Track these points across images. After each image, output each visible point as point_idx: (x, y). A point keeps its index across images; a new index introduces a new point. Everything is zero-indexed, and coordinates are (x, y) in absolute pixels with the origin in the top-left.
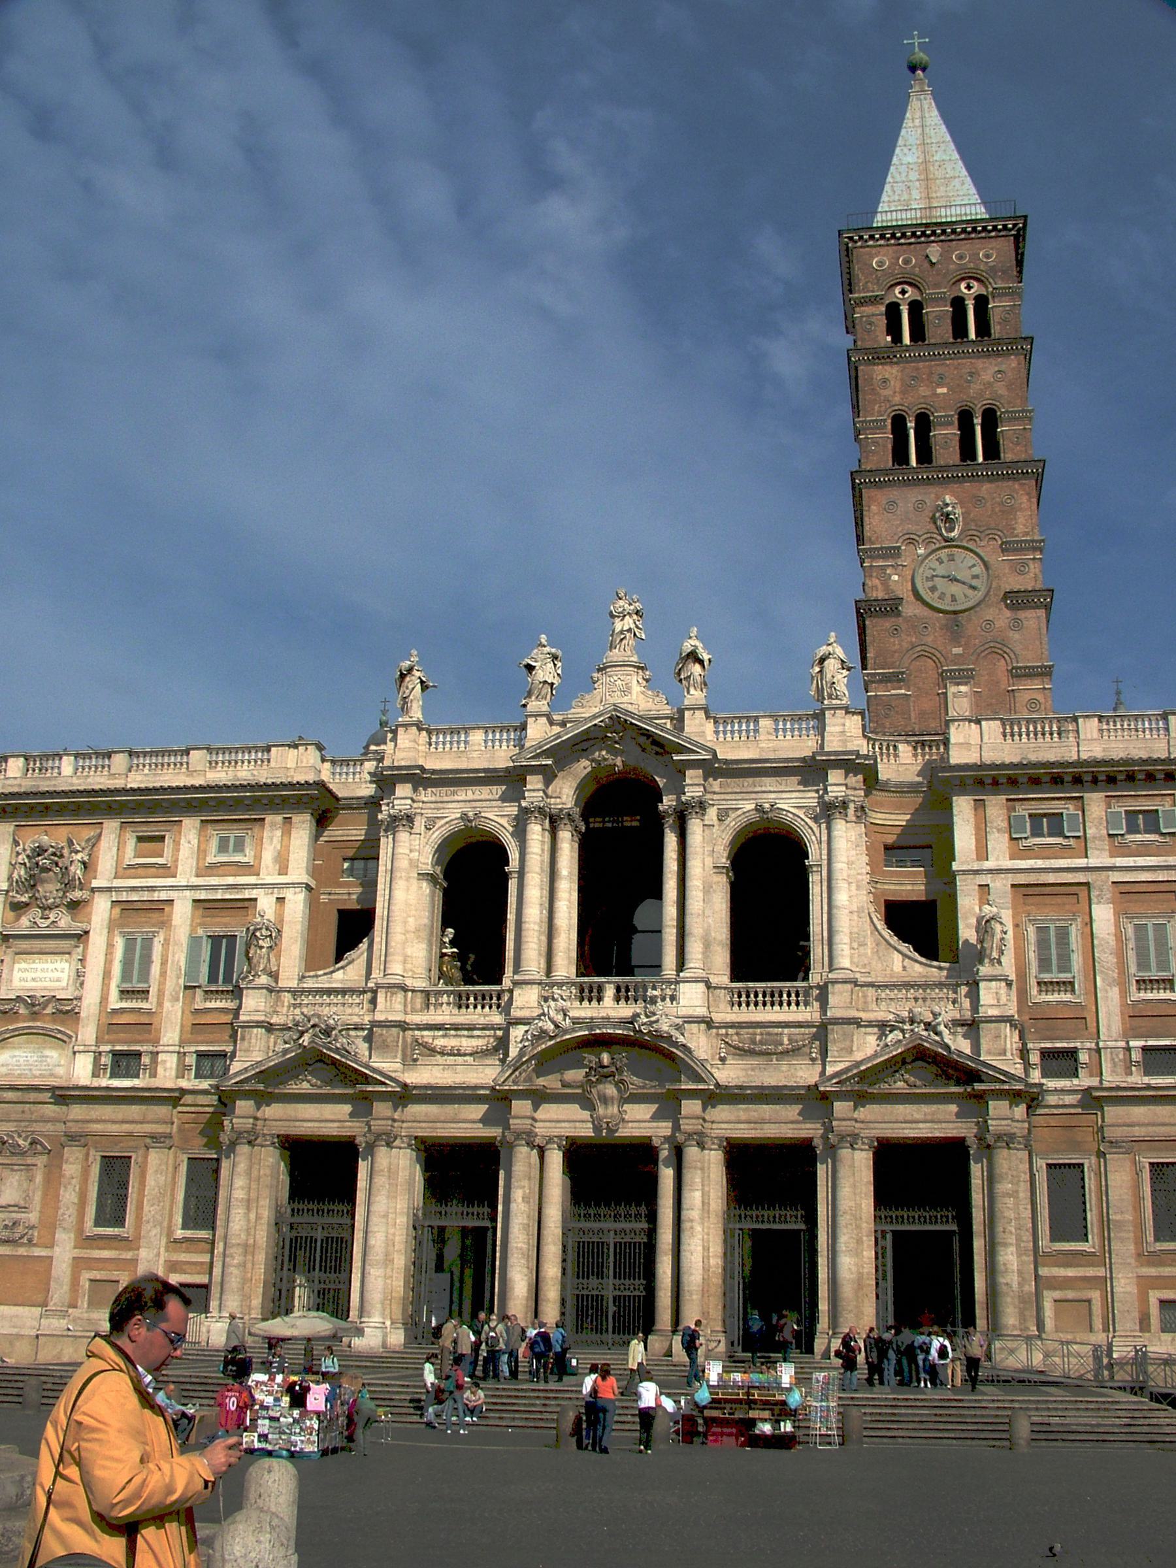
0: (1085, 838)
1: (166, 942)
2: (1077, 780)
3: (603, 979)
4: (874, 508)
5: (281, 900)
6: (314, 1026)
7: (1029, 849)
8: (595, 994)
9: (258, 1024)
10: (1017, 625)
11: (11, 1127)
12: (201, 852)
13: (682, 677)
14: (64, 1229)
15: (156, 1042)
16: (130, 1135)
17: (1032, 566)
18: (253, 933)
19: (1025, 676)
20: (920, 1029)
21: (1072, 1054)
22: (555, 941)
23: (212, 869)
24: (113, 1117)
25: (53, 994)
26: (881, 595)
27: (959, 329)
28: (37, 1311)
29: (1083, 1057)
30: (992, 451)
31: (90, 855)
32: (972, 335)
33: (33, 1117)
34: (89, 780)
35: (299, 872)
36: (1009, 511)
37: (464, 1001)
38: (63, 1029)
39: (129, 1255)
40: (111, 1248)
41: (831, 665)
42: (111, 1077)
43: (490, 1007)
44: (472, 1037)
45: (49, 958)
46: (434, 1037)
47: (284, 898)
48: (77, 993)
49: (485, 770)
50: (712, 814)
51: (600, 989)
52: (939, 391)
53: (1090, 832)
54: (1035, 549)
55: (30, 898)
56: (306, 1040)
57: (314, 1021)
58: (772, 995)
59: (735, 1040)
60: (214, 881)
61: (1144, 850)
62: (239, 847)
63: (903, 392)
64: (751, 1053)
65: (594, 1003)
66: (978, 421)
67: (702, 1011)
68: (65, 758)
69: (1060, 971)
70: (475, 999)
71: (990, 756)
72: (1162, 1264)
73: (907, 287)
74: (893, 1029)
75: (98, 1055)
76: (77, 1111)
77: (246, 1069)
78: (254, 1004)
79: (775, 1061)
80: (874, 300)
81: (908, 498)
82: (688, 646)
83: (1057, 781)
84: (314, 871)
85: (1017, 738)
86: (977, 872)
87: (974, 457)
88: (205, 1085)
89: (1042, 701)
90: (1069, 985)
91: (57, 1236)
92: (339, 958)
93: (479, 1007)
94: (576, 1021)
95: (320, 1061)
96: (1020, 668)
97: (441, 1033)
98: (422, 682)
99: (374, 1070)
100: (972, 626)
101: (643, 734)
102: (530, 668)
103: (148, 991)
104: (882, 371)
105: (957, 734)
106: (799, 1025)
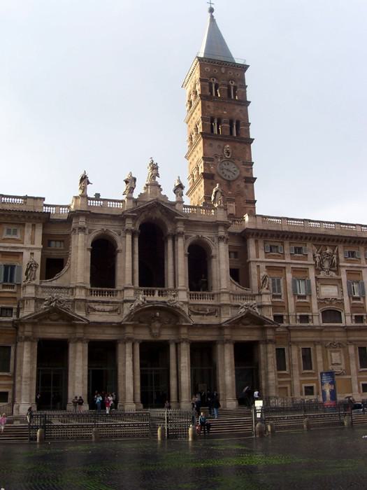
2: (283, 237)
3: (154, 288)
5: (32, 254)
6: (56, 300)
9: (33, 298)
10: (246, 187)
18: (31, 266)
20: (251, 309)
21: (281, 317)
23: (4, 239)
26: (208, 172)
29: (285, 318)
32: (233, 97)
35: (38, 244)
41: (219, 194)
52: (225, 112)
53: (286, 252)
56: (53, 304)
59: (192, 309)
60: (7, 245)
61: (298, 258)
62: (15, 233)
63: (214, 111)
64: (198, 314)
66: (235, 124)
67: (186, 300)
71: (259, 227)
74: (242, 307)
77: (31, 315)
78: (30, 292)
80: (206, 81)
81: (216, 144)
83: (278, 236)
84: (43, 243)
86: (256, 262)
90: (280, 297)
94: (148, 302)
99: (78, 316)
104: (208, 103)
106: (212, 305)
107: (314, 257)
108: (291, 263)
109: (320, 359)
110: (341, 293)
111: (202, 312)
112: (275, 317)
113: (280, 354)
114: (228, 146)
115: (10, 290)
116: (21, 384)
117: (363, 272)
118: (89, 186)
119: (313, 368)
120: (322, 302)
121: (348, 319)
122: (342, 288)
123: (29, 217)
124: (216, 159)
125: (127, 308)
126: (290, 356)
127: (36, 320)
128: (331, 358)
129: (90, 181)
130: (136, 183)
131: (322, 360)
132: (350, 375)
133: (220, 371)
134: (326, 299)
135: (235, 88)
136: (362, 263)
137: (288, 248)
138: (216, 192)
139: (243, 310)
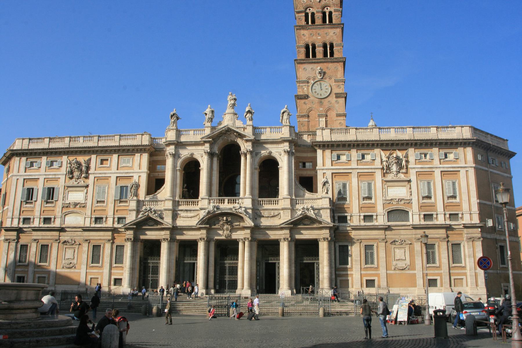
0: (351, 160)
4: (300, 70)
6: (149, 210)
7: (336, 163)
8: (223, 201)
9: (134, 210)
11: (69, 238)
13: (246, 117)
14: (84, 264)
15: (107, 214)
16: (100, 240)
17: (342, 86)
19: (339, 116)
22: (213, 187)
24: (96, 235)
25: (78, 202)
26: (301, 94)
27: (324, 21)
28: (77, 286)
30: (332, 54)
32: (327, 22)
33: (75, 235)
34: (87, 144)
36: (337, 70)
37: (188, 203)
39: (101, 271)
40: (96, 269)
41: (285, 114)
42: (95, 224)
43: (196, 205)
45: (78, 192)
46: (181, 213)
49: (195, 142)
50: (254, 153)
51: (224, 201)
52: (318, 38)
54: (342, 82)
56: (147, 213)
57: (148, 209)
58: (269, 202)
60: (122, 171)
61: (367, 163)
62: (128, 162)
63: (309, 38)
65: (223, 203)
66: (328, 46)
68: (81, 138)
70: (192, 203)
72: (367, 271)
73: (311, 9)
74: (300, 210)
76: (86, 233)
77: (131, 222)
79: (269, 219)
81: (309, 67)
82: (247, 110)
85: (334, 134)
86: (323, 169)
87: (327, 56)
88: (120, 226)
89: (343, 123)
92: (156, 192)
93: (193, 205)
95: (151, 220)
96: (338, 114)
97: (182, 212)
98: (177, 118)
100: (325, 102)
101: (236, 132)
102: (206, 114)
104: (303, 32)
105: (319, 132)
106: (276, 210)
107: (382, 162)
109: (382, 254)
110: (409, 193)
111: (267, 216)
114: (319, 68)
119: (376, 263)
121: (416, 218)
122: (410, 188)
124: (310, 81)
125: (202, 214)
127: (135, 227)
129: (180, 118)
132: (415, 269)
133: (281, 264)
134: (391, 200)
135: (330, 13)
136: (435, 164)
137: (354, 154)
138: (283, 113)
139: (300, 212)
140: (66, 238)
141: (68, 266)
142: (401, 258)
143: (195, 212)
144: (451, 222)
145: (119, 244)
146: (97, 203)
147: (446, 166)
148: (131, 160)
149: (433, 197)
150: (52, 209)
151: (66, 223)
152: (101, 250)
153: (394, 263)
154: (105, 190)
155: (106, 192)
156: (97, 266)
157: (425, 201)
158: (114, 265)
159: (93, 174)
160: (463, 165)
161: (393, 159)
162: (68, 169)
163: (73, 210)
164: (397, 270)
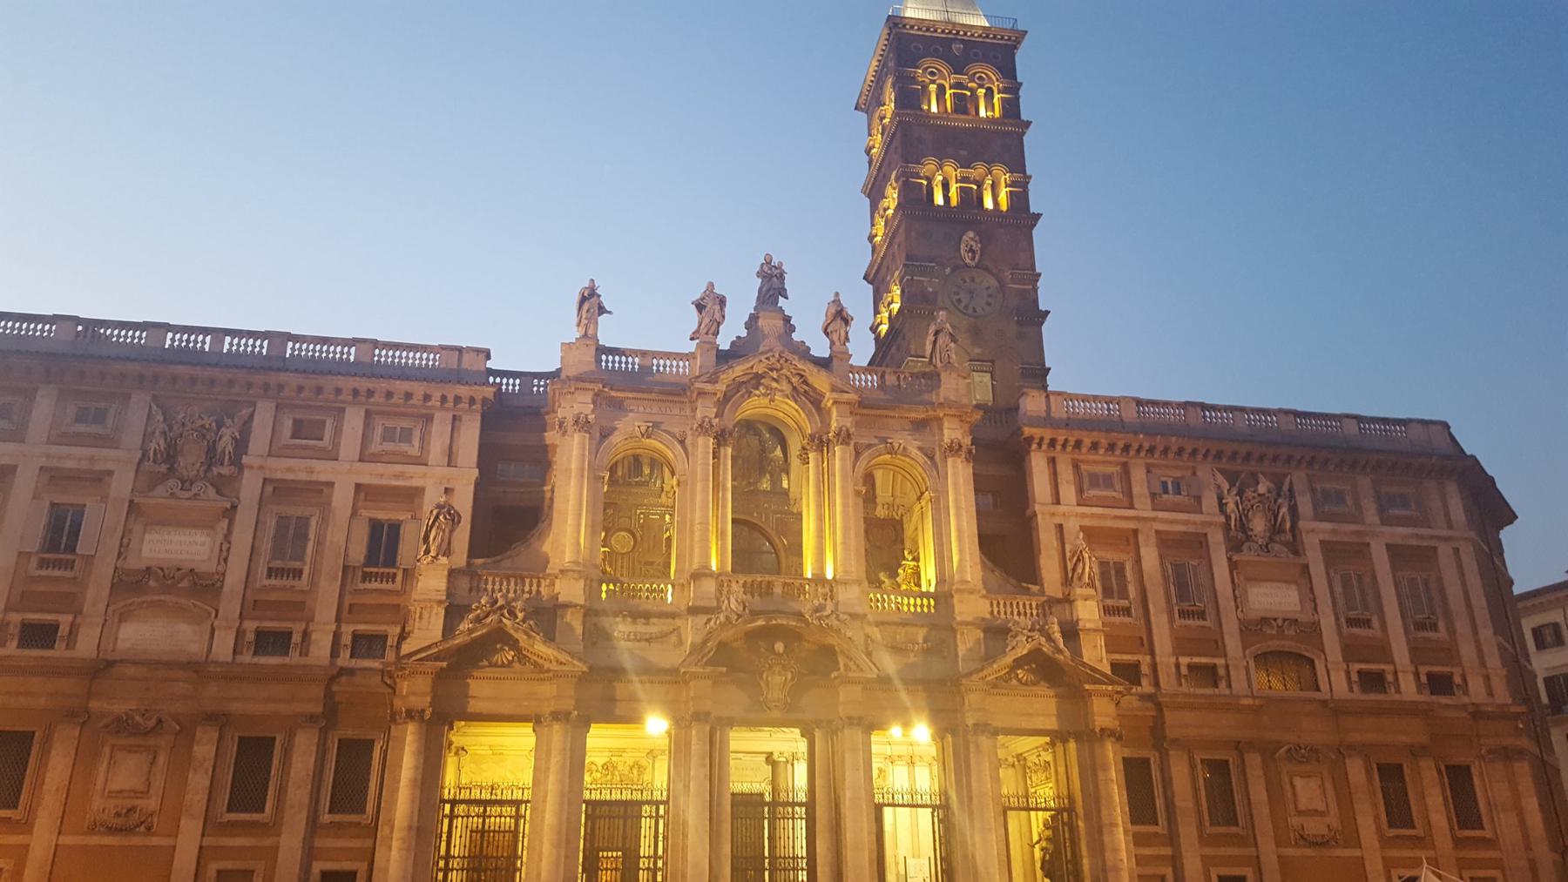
1: (324, 522)
6: (501, 608)
12: (365, 440)
13: (829, 330)
15: (310, 620)
31: (241, 433)
38: (198, 603)
39: (268, 842)
42: (255, 654)
44: (647, 624)
47: (452, 490)
48: (220, 568)
55: (171, 469)
62: (406, 436)
69: (1120, 598)
75: (240, 633)
77: (429, 647)
91: (182, 822)
103: (301, 571)
107: (1222, 506)
108: (1154, 519)
112: (1114, 666)
113: (1136, 773)
115: (384, 586)
116: (390, 848)
117: (1373, 545)
118: (602, 319)
120: (1253, 628)
123: (444, 399)
126: (1167, 782)
128: (1294, 794)
130: (727, 310)
131: (1264, 797)
134: (1264, 621)
140: (120, 708)
141: (119, 822)
142: (1313, 806)
143: (662, 620)
144: (1434, 698)
145: (350, 733)
146: (269, 576)
147: (1400, 533)
148: (417, 434)
149: (1375, 621)
150: (65, 588)
151: (121, 645)
152: (275, 761)
153: (1295, 821)
154: (307, 526)
155: (311, 536)
156: (254, 824)
157: (1355, 630)
158: (326, 818)
159: (261, 467)
160: (1444, 533)
161: (1254, 498)
162: (157, 443)
163: (162, 598)
164: (1304, 846)
